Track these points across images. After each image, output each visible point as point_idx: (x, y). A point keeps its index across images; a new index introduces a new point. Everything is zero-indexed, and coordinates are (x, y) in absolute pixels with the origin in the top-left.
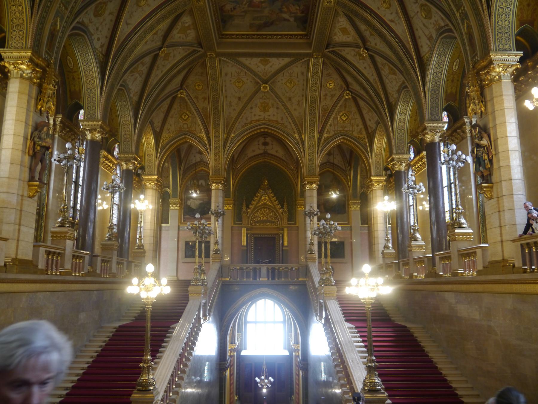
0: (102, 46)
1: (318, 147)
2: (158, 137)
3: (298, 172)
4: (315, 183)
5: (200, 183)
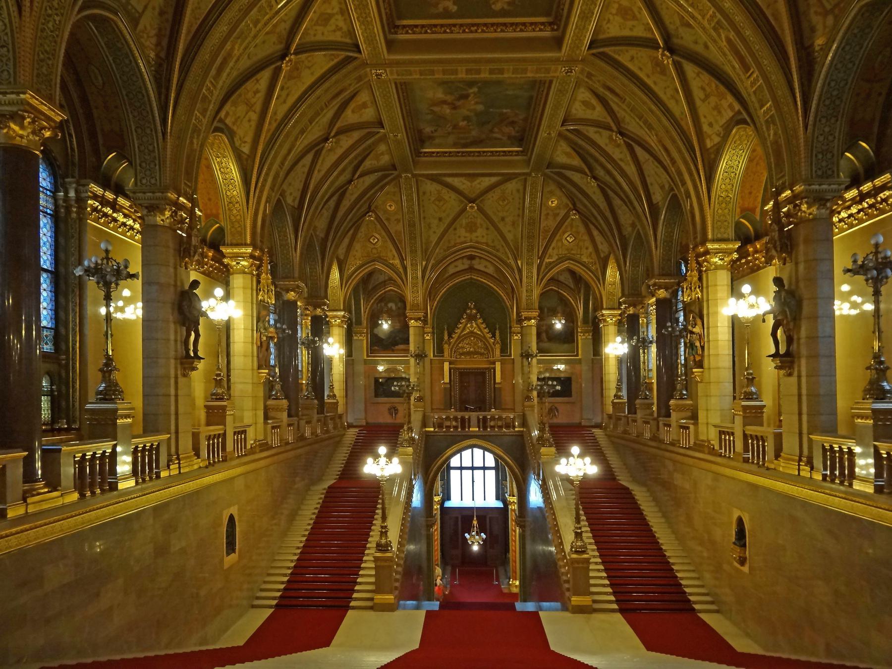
1: (538, 275)
4: (534, 318)
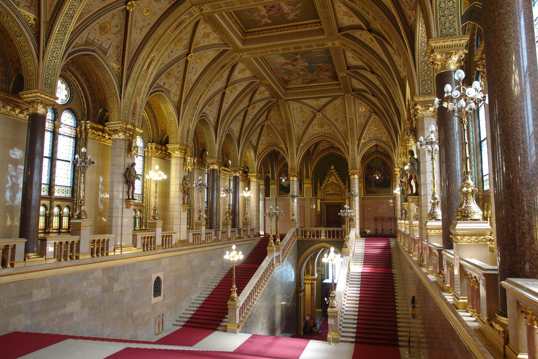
0: (214, 119)
1: (358, 150)
2: (255, 150)
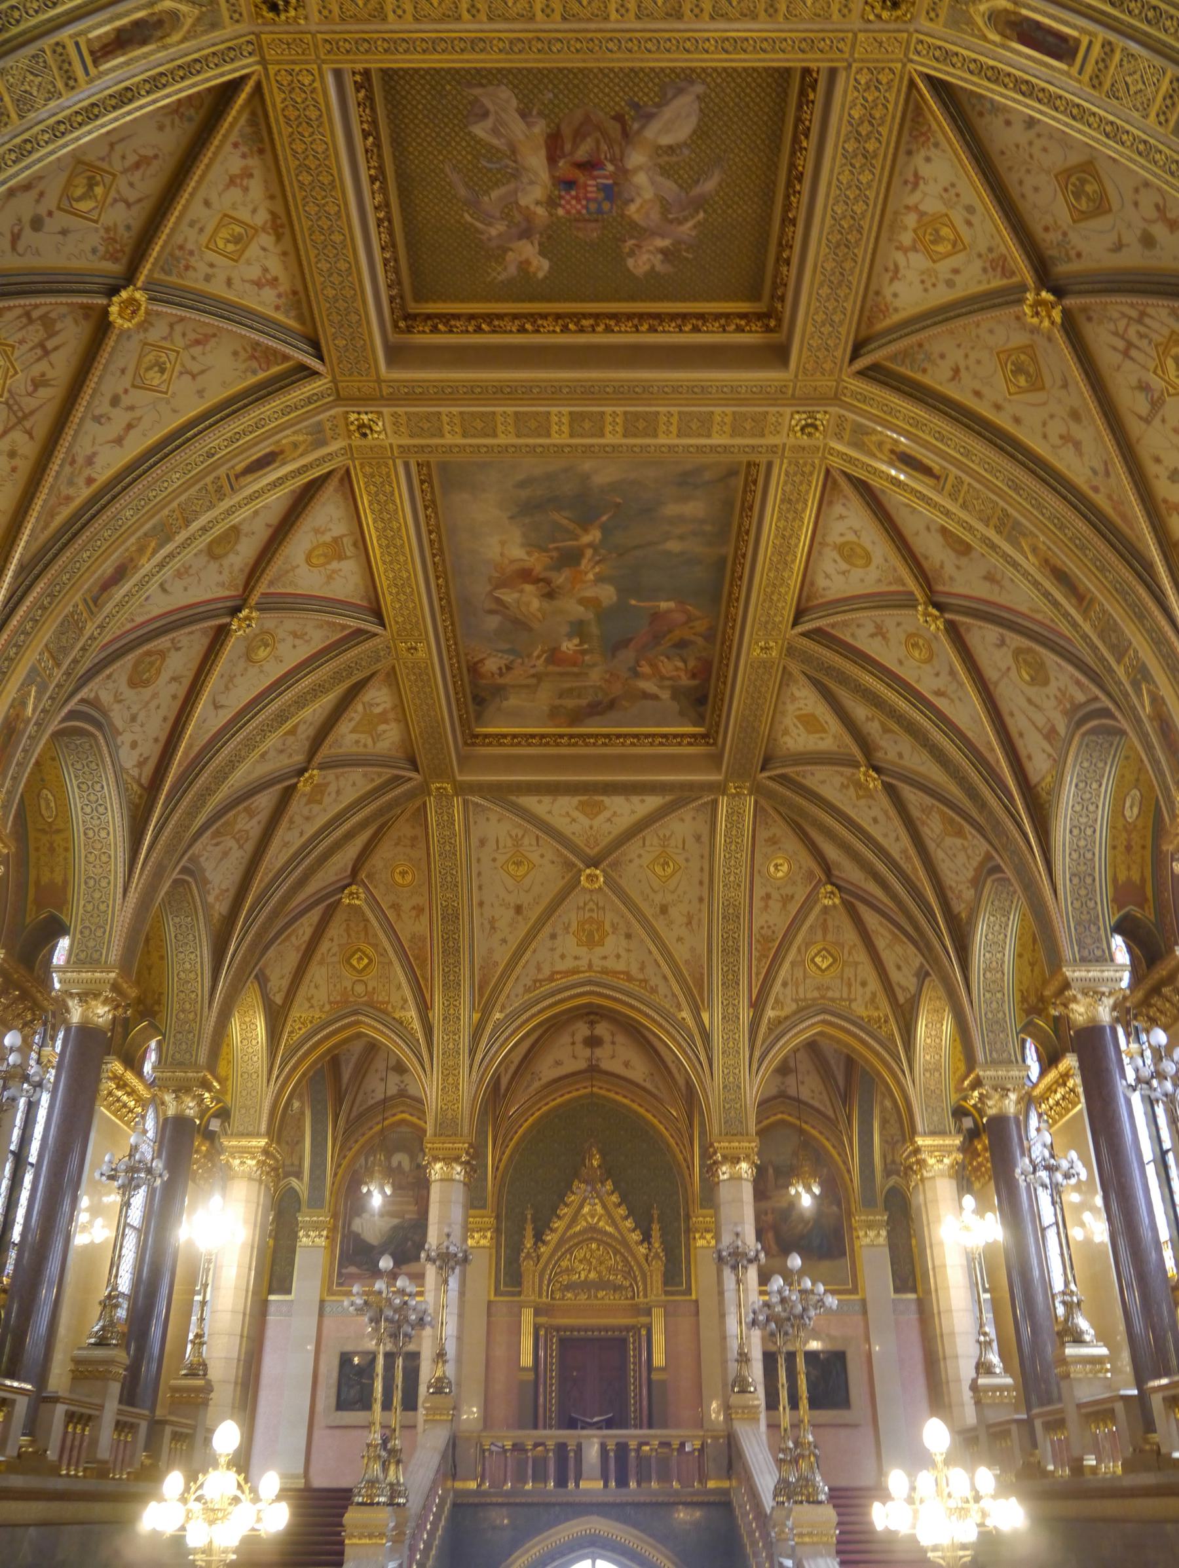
0: (141, 765)
3: (691, 1125)
4: (747, 1158)
5: (394, 1163)
